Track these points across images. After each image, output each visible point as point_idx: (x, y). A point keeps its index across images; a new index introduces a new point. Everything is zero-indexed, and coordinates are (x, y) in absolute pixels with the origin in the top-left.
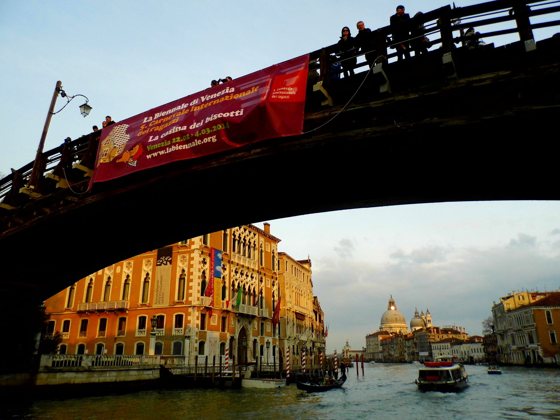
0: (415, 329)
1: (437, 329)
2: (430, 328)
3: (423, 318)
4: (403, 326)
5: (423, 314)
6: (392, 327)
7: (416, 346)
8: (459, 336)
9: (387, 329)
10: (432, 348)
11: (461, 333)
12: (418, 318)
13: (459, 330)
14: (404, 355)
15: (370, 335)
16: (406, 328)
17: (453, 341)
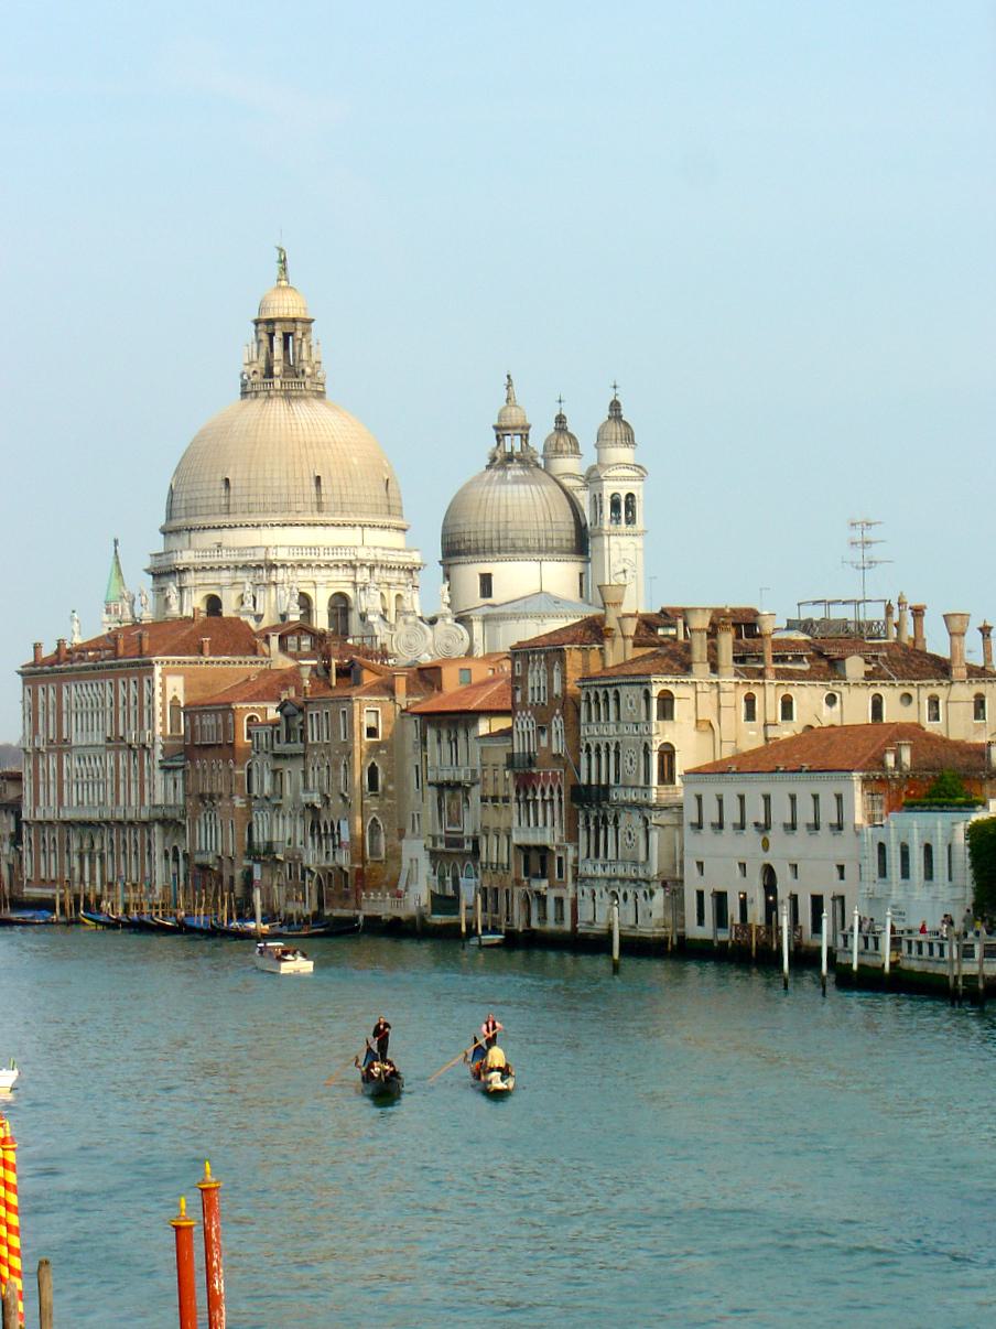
0: (486, 580)
1: (746, 624)
2: (667, 616)
3: (568, 482)
4: (380, 555)
5: (572, 437)
6: (272, 567)
7: (525, 782)
8: (934, 702)
9: (225, 576)
10: (691, 815)
11: (959, 672)
12: (516, 480)
13: (937, 643)
14: (395, 855)
15: (64, 654)
16: (403, 576)
17: (890, 760)
